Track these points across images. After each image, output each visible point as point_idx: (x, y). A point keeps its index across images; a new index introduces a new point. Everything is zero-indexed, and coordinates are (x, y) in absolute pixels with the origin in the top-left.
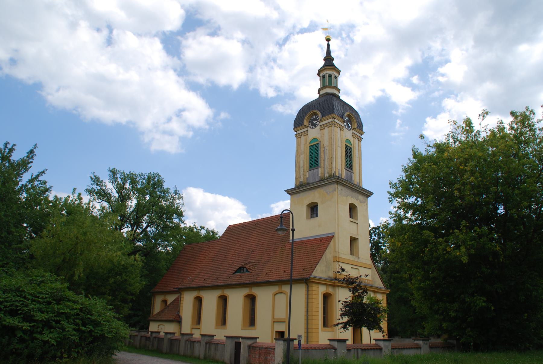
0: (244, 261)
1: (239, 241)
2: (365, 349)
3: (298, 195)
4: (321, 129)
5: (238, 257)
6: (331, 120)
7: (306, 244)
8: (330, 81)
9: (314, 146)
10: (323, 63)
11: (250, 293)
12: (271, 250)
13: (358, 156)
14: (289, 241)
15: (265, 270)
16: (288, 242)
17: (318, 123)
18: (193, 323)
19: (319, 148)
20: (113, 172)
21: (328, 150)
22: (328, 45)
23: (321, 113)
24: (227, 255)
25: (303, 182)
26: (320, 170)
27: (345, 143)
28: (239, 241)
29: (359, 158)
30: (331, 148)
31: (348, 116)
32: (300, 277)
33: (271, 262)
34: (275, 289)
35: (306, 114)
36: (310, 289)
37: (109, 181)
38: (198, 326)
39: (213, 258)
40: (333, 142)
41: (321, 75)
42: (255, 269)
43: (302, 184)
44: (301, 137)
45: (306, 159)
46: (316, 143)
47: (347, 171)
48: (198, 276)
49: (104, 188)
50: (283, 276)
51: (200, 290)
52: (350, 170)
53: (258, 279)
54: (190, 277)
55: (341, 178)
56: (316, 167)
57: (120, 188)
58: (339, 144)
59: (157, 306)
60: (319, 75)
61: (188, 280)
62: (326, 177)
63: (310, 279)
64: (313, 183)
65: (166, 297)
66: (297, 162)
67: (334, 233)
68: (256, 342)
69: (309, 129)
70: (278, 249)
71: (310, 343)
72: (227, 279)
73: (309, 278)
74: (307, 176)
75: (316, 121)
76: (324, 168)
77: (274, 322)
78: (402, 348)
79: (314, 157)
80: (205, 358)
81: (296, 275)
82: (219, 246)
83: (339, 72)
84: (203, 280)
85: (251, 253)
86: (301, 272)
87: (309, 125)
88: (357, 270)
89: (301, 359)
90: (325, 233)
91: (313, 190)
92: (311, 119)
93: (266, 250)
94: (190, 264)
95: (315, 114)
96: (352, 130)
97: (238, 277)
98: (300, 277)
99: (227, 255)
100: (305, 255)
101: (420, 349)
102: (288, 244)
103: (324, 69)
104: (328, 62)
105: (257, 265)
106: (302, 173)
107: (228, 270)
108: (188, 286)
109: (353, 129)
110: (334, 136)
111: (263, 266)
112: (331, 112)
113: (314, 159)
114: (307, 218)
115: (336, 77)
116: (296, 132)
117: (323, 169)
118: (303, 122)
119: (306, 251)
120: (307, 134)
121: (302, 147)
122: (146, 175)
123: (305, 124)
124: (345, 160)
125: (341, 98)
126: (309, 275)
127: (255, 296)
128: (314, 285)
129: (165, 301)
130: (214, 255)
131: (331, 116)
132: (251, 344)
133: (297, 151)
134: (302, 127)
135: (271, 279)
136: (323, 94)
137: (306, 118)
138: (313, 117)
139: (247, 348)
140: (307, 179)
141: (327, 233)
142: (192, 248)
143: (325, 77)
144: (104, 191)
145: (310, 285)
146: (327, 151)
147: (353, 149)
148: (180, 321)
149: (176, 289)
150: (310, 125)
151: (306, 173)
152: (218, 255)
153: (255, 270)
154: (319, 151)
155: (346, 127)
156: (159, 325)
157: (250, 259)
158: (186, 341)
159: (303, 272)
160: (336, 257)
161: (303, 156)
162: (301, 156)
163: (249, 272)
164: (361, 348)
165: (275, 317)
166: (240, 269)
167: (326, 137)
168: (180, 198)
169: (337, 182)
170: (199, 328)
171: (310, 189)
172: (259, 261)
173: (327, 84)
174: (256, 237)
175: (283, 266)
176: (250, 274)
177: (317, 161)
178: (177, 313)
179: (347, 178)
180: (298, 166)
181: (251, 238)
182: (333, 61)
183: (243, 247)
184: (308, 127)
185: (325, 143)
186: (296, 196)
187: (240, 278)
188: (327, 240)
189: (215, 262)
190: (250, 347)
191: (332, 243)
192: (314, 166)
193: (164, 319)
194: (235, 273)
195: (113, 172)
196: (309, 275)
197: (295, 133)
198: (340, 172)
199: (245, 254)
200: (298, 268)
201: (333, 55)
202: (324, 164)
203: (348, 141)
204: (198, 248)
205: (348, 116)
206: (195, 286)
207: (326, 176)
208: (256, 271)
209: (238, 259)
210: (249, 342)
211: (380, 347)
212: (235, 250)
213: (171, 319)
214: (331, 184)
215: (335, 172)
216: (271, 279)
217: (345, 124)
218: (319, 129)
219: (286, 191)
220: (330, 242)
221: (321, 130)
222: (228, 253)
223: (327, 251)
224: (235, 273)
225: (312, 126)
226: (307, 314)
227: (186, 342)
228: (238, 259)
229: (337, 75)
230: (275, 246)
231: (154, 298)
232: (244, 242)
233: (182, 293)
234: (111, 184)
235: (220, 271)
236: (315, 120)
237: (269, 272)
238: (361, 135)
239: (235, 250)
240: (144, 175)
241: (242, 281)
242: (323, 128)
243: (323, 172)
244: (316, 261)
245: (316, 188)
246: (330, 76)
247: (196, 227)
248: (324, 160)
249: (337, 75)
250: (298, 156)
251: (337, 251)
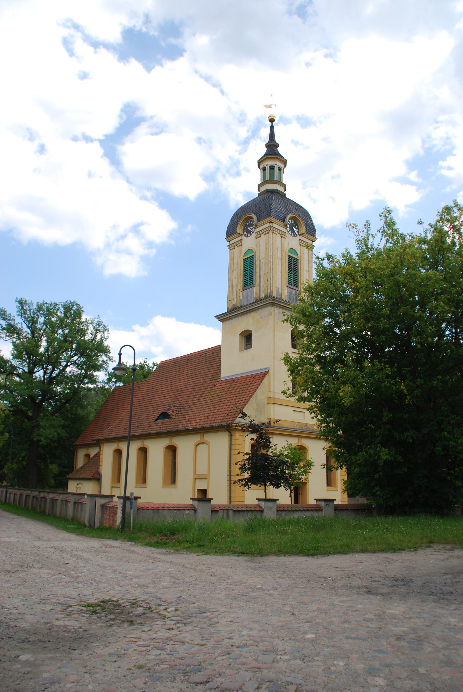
0: (170, 406)
1: (168, 380)
2: (239, 511)
3: (230, 321)
4: (257, 237)
5: (164, 400)
6: (267, 225)
7: (237, 382)
8: (272, 175)
9: (249, 259)
10: (264, 150)
11: (171, 444)
12: (199, 391)
13: (307, 270)
14: (220, 379)
15: (188, 416)
16: (218, 380)
17: (253, 229)
18: (113, 482)
19: (254, 262)
20: (21, 303)
21: (264, 263)
22: (272, 127)
23: (257, 216)
24: (153, 398)
25: (236, 304)
26: (255, 289)
27: (287, 253)
28: (168, 380)
29: (309, 271)
30: (267, 261)
31: (293, 218)
32: (222, 423)
33: (197, 405)
34: (196, 439)
35: (240, 217)
36: (233, 438)
37: (17, 314)
38: (118, 485)
39: (139, 403)
40: (269, 253)
41: (262, 166)
42: (179, 415)
43: (235, 308)
44: (234, 248)
45: (240, 276)
46: (251, 255)
47: (290, 289)
48: (120, 425)
49: (12, 322)
50: (205, 423)
51: (120, 441)
52: (295, 288)
53: (180, 426)
54: (112, 426)
55: (281, 299)
56: (251, 286)
57: (32, 322)
58: (279, 254)
59: (80, 461)
60: (259, 167)
61: (108, 430)
62: (262, 298)
63: (232, 426)
64: (246, 306)
65: (89, 451)
66: (230, 280)
67: (268, 368)
68: (112, 501)
69: (243, 237)
70: (207, 390)
71: (232, 503)
72: (148, 428)
73: (230, 425)
74: (241, 298)
75: (251, 228)
76: (259, 286)
77: (195, 478)
78: (293, 511)
79: (249, 273)
80: (73, 520)
81: (219, 421)
82: (147, 387)
83: (284, 162)
84: (124, 429)
85: (178, 395)
86: (225, 418)
87: (244, 232)
88: (302, 414)
89: (134, 521)
90: (259, 368)
91: (246, 315)
92: (246, 225)
93: (194, 391)
94: (117, 410)
95: (250, 218)
96: (299, 236)
97: (159, 424)
98: (222, 423)
99: (153, 398)
100: (233, 396)
101: (321, 512)
102: (219, 382)
103: (265, 159)
104: (270, 149)
105: (181, 410)
106: (235, 293)
107: (151, 417)
108: (107, 437)
109: (300, 235)
110: (271, 246)
111: (188, 411)
112: (268, 215)
113: (249, 275)
114: (240, 350)
115: (280, 169)
116: (229, 242)
117: (258, 288)
118: (236, 230)
119: (235, 391)
120: (241, 244)
121: (236, 260)
122: (60, 304)
123: (238, 231)
124: (287, 275)
125: (287, 196)
126: (232, 421)
127: (176, 448)
128: (238, 433)
129: (88, 455)
130: (139, 398)
131: (268, 219)
132: (105, 504)
133: (230, 266)
135: (192, 427)
136: (262, 192)
137: (240, 224)
138: (248, 222)
139: (100, 508)
140: (241, 301)
141: (261, 368)
142: (121, 391)
143: (265, 170)
144: (12, 326)
145: (233, 433)
146: (263, 265)
147: (299, 260)
148: (100, 479)
149: (95, 441)
150: (245, 233)
151: (240, 293)
152: (144, 399)
153: (178, 416)
154: (254, 265)
155: (290, 232)
156: (78, 484)
157: (175, 402)
158: (62, 501)
159: (227, 417)
160: (271, 398)
161: (236, 272)
162: (234, 272)
163: (171, 418)
164: (233, 509)
165: (197, 473)
166: (164, 415)
167: (263, 247)
168: (105, 330)
169: (273, 304)
170: (119, 487)
171: (243, 314)
172: (184, 405)
173: (268, 178)
174: (187, 375)
175: (208, 410)
176: (172, 420)
177: (251, 278)
178: (96, 470)
179: (290, 298)
180: (231, 286)
181: (181, 377)
182: (278, 149)
183: (170, 388)
184: (242, 235)
185: (261, 255)
186: (228, 323)
187: (161, 426)
188: (260, 377)
189: (140, 407)
190: (103, 507)
191: (265, 380)
192: (248, 284)
193: (82, 476)
194: (157, 420)
195: (21, 303)
196: (232, 421)
197: (228, 244)
198: (280, 291)
199: (172, 396)
200: (222, 413)
201: (278, 139)
202: (260, 282)
203: (292, 250)
204: (128, 390)
205: (293, 218)
206: (113, 436)
207: (261, 297)
208: (180, 417)
209: (164, 402)
210: (103, 501)
211: (261, 508)
212: (162, 392)
213: (89, 476)
214: (266, 306)
215: (272, 291)
216: (192, 427)
217: (288, 229)
218: (255, 237)
219: (215, 316)
220: (263, 379)
221: (256, 238)
222: (154, 395)
223: (258, 390)
224: (157, 420)
225: (247, 234)
226: (230, 468)
227: (62, 502)
228: (164, 402)
229: (282, 166)
230: (204, 385)
231: (77, 452)
232: (173, 381)
233: (102, 445)
234: (20, 317)
235: (143, 418)
236: (251, 225)
237: (192, 417)
238: (313, 242)
239: (162, 392)
240: (59, 305)
241: (163, 429)
242: (259, 236)
243: (258, 291)
244: (243, 404)
245: (250, 312)
246: (272, 168)
247: (147, 364)
248: (260, 277)
249: (282, 166)
250: (231, 271)
251: (272, 390)
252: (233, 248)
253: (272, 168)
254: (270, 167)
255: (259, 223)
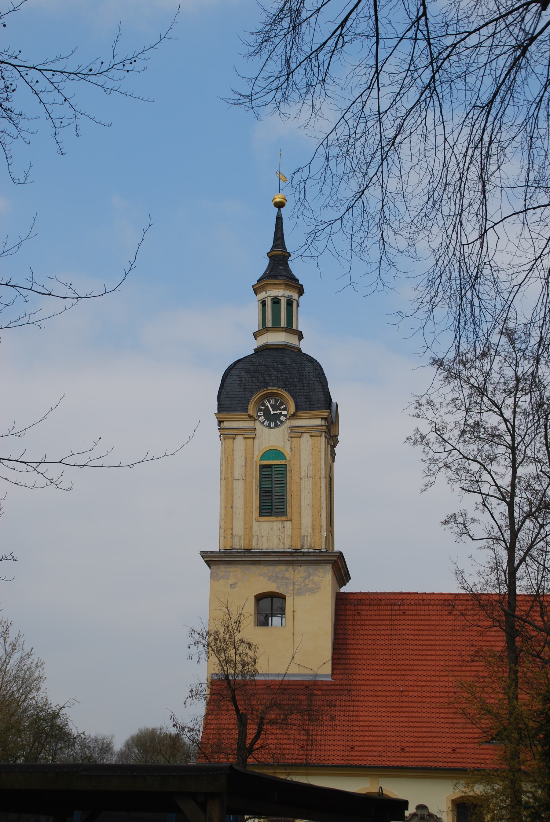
69: (258, 425)
120: (253, 436)
134: (244, 415)
143: (265, 304)
150: (262, 418)
221: (291, 437)
246: (276, 301)
252: (232, 436)
253: (276, 301)
254: (272, 299)
255: (300, 414)
